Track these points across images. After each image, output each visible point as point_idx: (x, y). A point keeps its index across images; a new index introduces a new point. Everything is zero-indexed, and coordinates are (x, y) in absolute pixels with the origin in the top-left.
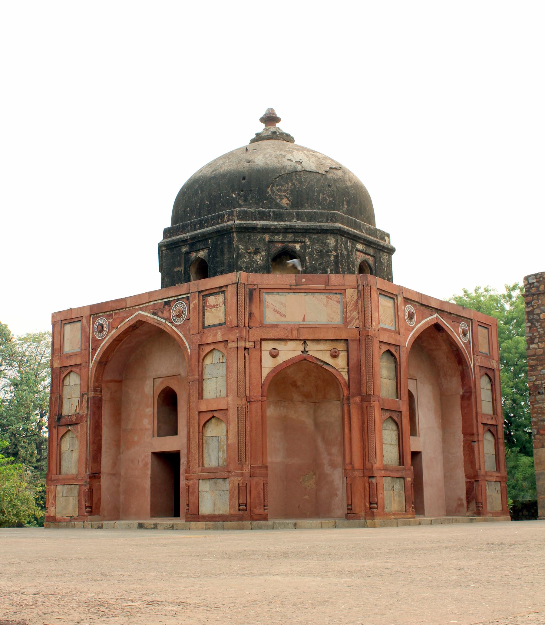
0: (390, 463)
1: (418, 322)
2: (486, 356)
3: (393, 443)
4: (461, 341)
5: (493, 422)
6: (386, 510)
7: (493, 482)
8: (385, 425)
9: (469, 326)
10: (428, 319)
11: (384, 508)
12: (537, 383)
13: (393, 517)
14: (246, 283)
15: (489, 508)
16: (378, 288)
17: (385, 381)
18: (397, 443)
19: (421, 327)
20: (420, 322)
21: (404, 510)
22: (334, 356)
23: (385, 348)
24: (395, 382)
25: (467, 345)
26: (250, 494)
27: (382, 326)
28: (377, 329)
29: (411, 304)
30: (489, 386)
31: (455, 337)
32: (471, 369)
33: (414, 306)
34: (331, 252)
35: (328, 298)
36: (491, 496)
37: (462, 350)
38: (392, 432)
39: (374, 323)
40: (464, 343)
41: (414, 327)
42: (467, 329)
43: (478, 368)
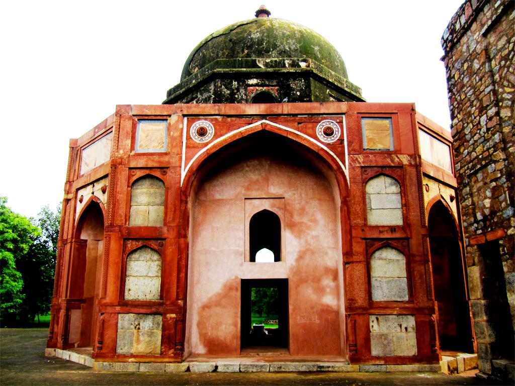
0: (141, 297)
1: (216, 136)
2: (388, 153)
3: (150, 274)
4: (319, 141)
5: (397, 235)
6: (119, 351)
7: (394, 316)
8: (136, 256)
9: (341, 123)
10: (242, 129)
11: (114, 349)
12: (462, 172)
13: (130, 360)
14: (75, 146)
15: (375, 352)
16: (134, 115)
17: (143, 208)
18: (160, 275)
19: (226, 140)
20: (221, 135)
21: (158, 351)
22: (104, 192)
23: (139, 174)
24: (163, 208)
25: (338, 147)
26: (58, 324)
27: (139, 149)
28: (126, 156)
29: (206, 119)
30: (395, 189)
31: (305, 139)
32: (343, 173)
33: (211, 120)
34: (211, 96)
35: (107, 139)
36: (383, 336)
37: (321, 153)
38: (150, 262)
39: (121, 152)
40: (328, 145)
41: (206, 144)
42: (335, 127)
43: (358, 171)
